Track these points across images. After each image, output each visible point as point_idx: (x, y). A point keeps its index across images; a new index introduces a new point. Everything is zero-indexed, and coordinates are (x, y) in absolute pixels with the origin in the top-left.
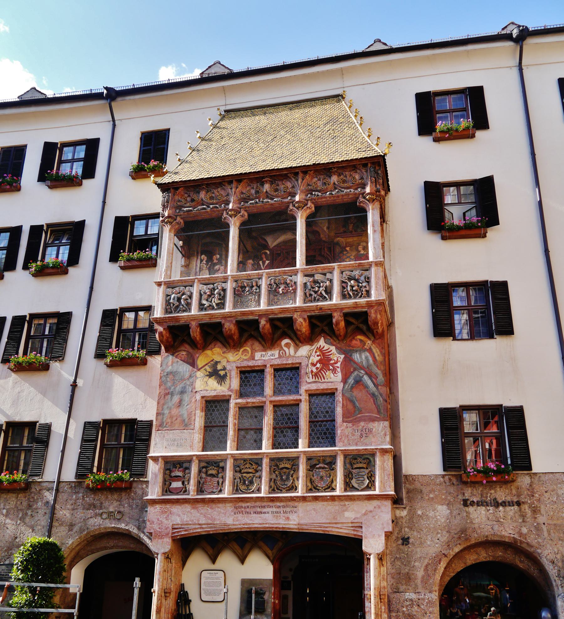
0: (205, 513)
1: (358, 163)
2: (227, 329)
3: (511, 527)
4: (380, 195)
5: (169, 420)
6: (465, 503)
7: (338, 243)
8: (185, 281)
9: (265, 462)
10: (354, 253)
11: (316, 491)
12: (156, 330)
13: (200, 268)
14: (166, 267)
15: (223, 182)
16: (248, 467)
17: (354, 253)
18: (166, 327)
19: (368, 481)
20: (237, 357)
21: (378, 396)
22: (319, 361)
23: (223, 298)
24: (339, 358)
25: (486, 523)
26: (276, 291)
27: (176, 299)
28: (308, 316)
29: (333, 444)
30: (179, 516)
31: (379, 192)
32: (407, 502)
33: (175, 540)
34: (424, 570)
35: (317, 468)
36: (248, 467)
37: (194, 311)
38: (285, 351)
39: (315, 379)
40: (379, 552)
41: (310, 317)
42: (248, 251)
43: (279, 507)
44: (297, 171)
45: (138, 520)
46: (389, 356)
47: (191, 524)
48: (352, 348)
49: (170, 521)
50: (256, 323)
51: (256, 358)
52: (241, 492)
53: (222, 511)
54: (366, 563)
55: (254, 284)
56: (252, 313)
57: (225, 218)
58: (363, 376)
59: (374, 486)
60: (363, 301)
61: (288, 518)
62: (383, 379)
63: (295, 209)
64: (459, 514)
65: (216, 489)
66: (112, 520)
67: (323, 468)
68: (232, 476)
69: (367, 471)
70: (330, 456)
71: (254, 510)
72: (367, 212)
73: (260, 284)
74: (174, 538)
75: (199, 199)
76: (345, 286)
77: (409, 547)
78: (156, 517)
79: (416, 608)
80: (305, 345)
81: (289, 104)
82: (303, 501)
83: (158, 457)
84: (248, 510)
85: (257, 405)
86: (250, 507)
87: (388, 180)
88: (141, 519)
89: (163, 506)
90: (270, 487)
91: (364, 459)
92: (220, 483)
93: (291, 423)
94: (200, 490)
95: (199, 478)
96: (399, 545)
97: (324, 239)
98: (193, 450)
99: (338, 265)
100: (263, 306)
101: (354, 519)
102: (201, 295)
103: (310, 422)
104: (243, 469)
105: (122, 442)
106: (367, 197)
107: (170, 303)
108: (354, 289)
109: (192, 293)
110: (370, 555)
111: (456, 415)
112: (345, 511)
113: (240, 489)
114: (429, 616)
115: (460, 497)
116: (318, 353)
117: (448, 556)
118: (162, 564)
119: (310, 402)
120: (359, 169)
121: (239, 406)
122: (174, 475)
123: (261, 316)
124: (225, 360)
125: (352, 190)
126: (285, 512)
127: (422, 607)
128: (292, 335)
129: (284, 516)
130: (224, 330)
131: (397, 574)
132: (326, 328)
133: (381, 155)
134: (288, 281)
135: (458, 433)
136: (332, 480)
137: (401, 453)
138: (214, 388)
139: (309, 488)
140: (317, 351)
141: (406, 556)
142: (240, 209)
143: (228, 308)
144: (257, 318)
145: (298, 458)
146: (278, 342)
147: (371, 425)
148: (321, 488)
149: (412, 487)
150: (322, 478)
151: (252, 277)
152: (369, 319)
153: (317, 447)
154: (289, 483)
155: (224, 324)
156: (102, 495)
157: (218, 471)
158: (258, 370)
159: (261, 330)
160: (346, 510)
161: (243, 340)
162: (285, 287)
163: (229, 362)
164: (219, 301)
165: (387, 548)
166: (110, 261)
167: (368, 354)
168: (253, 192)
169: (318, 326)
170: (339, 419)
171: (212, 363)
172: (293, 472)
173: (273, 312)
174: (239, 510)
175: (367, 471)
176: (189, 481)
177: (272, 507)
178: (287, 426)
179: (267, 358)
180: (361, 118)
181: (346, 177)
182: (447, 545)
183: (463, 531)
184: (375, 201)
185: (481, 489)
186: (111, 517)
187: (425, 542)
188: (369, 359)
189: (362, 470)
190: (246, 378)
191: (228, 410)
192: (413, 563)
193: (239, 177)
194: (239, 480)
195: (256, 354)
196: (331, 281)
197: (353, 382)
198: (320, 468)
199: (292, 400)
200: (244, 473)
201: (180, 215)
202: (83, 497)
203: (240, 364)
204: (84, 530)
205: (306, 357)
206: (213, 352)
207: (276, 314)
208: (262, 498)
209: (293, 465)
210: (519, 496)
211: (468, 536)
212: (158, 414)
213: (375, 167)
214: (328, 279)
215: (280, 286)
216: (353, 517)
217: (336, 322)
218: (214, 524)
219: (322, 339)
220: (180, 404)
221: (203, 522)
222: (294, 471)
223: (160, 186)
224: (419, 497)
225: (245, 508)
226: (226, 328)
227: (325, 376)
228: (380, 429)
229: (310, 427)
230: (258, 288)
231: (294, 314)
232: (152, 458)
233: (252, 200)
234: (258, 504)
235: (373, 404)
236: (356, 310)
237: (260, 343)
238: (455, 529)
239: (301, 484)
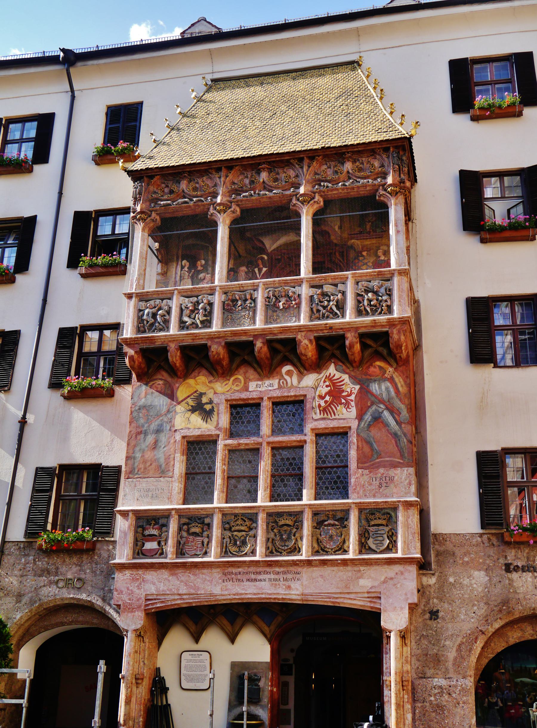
0: (187, 581)
1: (378, 147)
2: (214, 353)
4: (404, 187)
5: (142, 466)
6: (508, 568)
7: (352, 247)
8: (162, 292)
9: (261, 518)
10: (372, 259)
11: (324, 553)
12: (126, 354)
13: (181, 277)
14: (139, 275)
15: (210, 169)
16: (239, 523)
17: (372, 259)
18: (138, 350)
19: (388, 541)
20: (227, 388)
21: (401, 436)
22: (329, 393)
23: (209, 314)
24: (353, 389)
25: (533, 593)
26: (275, 306)
27: (150, 315)
28: (315, 338)
29: (346, 496)
30: (154, 584)
31: (404, 183)
32: (436, 567)
33: (148, 614)
34: (457, 651)
35: (325, 526)
37: (173, 330)
38: (286, 380)
39: (324, 415)
40: (401, 629)
41: (317, 339)
42: (240, 256)
43: (278, 573)
44: (302, 156)
45: (103, 589)
46: (415, 387)
47: (168, 594)
48: (369, 378)
49: (142, 590)
50: (250, 345)
51: (250, 390)
52: (231, 555)
53: (208, 578)
54: (385, 641)
55: (248, 297)
56: (245, 332)
57: (212, 215)
58: (383, 411)
59: (396, 547)
60: (383, 318)
61: (289, 587)
62: (407, 415)
63: (299, 203)
64: (500, 582)
65: (201, 551)
66: (71, 589)
68: (219, 535)
69: (387, 529)
70: (342, 511)
71: (247, 577)
72: (388, 208)
73: (256, 296)
74: (147, 612)
75: (179, 190)
76: (361, 300)
77: (438, 623)
78: (125, 585)
79: (446, 697)
80: (311, 373)
81: (292, 73)
82: (307, 566)
83: (128, 511)
84: (239, 577)
85: (251, 447)
86: (242, 573)
87: (414, 169)
88: (106, 588)
89: (134, 572)
90: (267, 548)
91: (384, 514)
92: (205, 543)
93: (294, 469)
94: (180, 552)
95: (179, 538)
96: (426, 619)
97: (335, 241)
98: (171, 503)
99: (353, 274)
100: (259, 324)
101: (371, 588)
102: (182, 310)
103: (316, 468)
104: (233, 526)
105: (84, 492)
106: (389, 189)
107: (143, 320)
108: (372, 303)
109: (170, 308)
110: (390, 632)
111: (498, 460)
112: (360, 578)
113: (230, 551)
114: (463, 707)
115: (502, 561)
116: (327, 383)
117: (486, 633)
118: (133, 644)
119: (317, 444)
120: (379, 155)
121: (229, 448)
122: (148, 533)
123: (256, 337)
124: (212, 391)
125: (370, 180)
126: (286, 580)
127: (454, 695)
128: (295, 360)
130: (210, 353)
131: (424, 655)
132: (337, 353)
133: (405, 137)
134: (290, 294)
135: (499, 482)
137: (429, 507)
138: (198, 426)
139: (315, 550)
140: (326, 380)
141: (434, 633)
142: (231, 202)
143: (216, 327)
144: (252, 339)
145: (301, 513)
146: (278, 369)
147: (392, 472)
148: (330, 550)
149: (442, 549)
150: (331, 537)
151: (245, 288)
152: (391, 340)
153: (326, 499)
155: (210, 347)
156: (58, 558)
157: (203, 529)
158: (252, 404)
159: (256, 353)
161: (234, 366)
162: (287, 301)
164: (205, 318)
165: (411, 623)
166: (68, 267)
167: (389, 384)
168: (247, 181)
169: (327, 350)
170: (353, 464)
171: (195, 394)
172: (295, 530)
173: (271, 332)
174: (229, 576)
175: (387, 529)
176: (166, 540)
177: (270, 573)
178: (288, 473)
180: (382, 90)
181: (362, 163)
182: (485, 619)
183: (505, 602)
184: (399, 194)
185: (527, 551)
186: (70, 586)
187: (458, 616)
188: (390, 391)
189: (381, 528)
190: (238, 413)
191: (215, 453)
192: (443, 642)
193: (230, 163)
195: (250, 383)
196: (344, 293)
197: (370, 418)
198: (329, 525)
199: (295, 441)
200: (235, 531)
201: (156, 211)
202: (34, 560)
203: (231, 396)
204: (35, 602)
205: (312, 388)
206: (196, 381)
207: (275, 334)
208: (256, 563)
209: (295, 522)
211: (510, 609)
212: (127, 458)
213: (399, 152)
214: (340, 291)
215: (281, 299)
216: (370, 585)
217: (350, 344)
218: (198, 594)
219: (333, 365)
220: (155, 445)
221: (185, 592)
222: (297, 529)
223: (130, 173)
224: (451, 561)
225: (236, 574)
226: (213, 352)
229: (317, 474)
230: (252, 302)
231: (298, 335)
232: (120, 512)
233: (246, 192)
234: (252, 569)
235: (395, 446)
236: (374, 330)
237: (255, 370)
238: (495, 600)
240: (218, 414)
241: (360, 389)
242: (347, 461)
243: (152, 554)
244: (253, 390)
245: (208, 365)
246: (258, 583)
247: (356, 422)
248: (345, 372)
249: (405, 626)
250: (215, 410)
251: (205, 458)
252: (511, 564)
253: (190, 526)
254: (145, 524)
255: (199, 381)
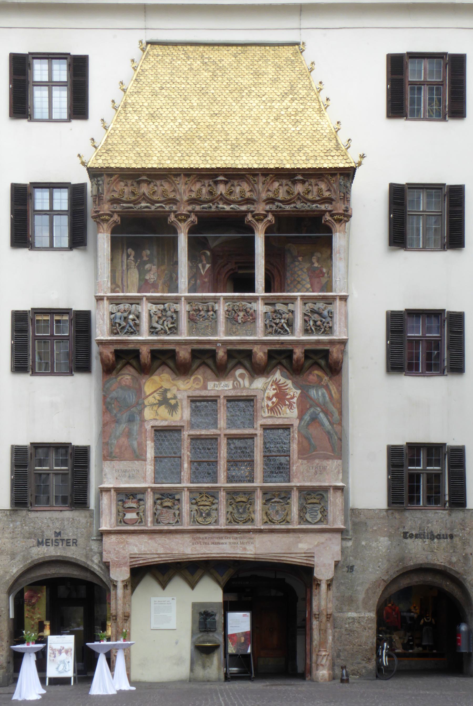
3: (443, 557)
11: (272, 523)
20: (189, 386)
22: (276, 395)
24: (295, 393)
30: (136, 546)
35: (272, 502)
36: (204, 500)
39: (271, 413)
40: (328, 579)
43: (236, 538)
47: (148, 554)
49: (127, 550)
53: (180, 542)
58: (319, 413)
61: (245, 549)
65: (173, 520)
67: (278, 502)
69: (320, 506)
70: (286, 492)
71: (212, 541)
74: (132, 567)
80: (260, 377)
84: (205, 541)
89: (119, 536)
91: (318, 495)
92: (177, 514)
94: (157, 521)
98: (145, 481)
101: (307, 550)
103: (264, 456)
116: (274, 387)
122: (128, 506)
124: (175, 387)
126: (243, 543)
129: (241, 547)
132: (284, 361)
136: (287, 513)
139: (265, 521)
140: (273, 384)
146: (232, 371)
150: (277, 512)
154: (245, 516)
160: (300, 542)
163: (180, 390)
167: (325, 391)
171: (161, 390)
174: (197, 540)
175: (320, 506)
176: (144, 511)
177: (230, 538)
179: (220, 389)
189: (316, 505)
191: (180, 440)
194: (196, 512)
195: (209, 383)
197: (309, 418)
198: (275, 502)
209: (249, 499)
210: (452, 529)
221: (162, 552)
222: (250, 505)
225: (203, 539)
227: (281, 411)
228: (334, 467)
234: (216, 535)
239: (258, 516)
240: (182, 408)
241: (301, 393)
242: (289, 451)
243: (133, 522)
244: (211, 389)
245: (172, 364)
246: (221, 545)
247: (298, 421)
248: (289, 379)
249: (331, 577)
250: (179, 404)
251: (170, 444)
252: (407, 532)
253: (163, 501)
254: (124, 499)
255: (163, 378)
